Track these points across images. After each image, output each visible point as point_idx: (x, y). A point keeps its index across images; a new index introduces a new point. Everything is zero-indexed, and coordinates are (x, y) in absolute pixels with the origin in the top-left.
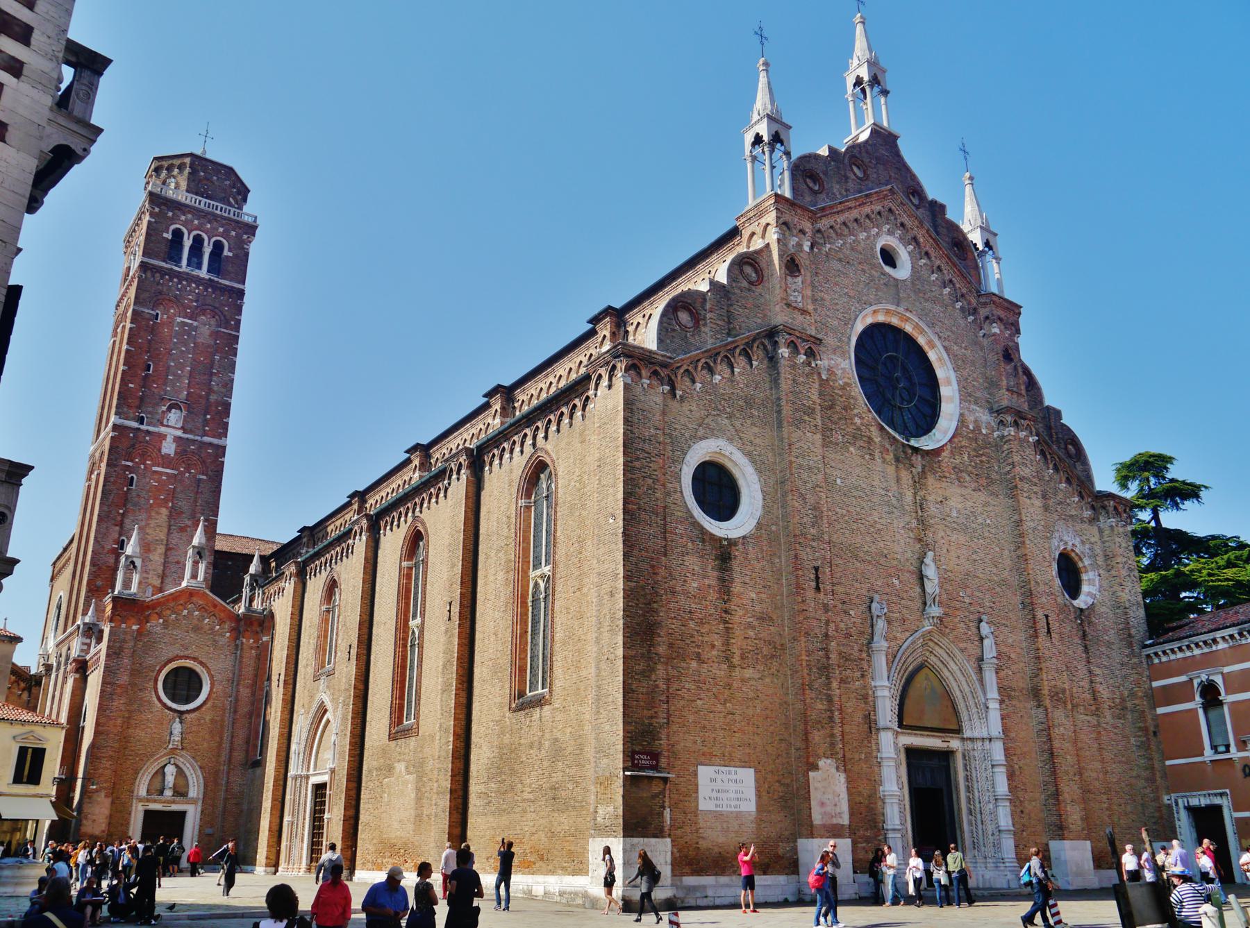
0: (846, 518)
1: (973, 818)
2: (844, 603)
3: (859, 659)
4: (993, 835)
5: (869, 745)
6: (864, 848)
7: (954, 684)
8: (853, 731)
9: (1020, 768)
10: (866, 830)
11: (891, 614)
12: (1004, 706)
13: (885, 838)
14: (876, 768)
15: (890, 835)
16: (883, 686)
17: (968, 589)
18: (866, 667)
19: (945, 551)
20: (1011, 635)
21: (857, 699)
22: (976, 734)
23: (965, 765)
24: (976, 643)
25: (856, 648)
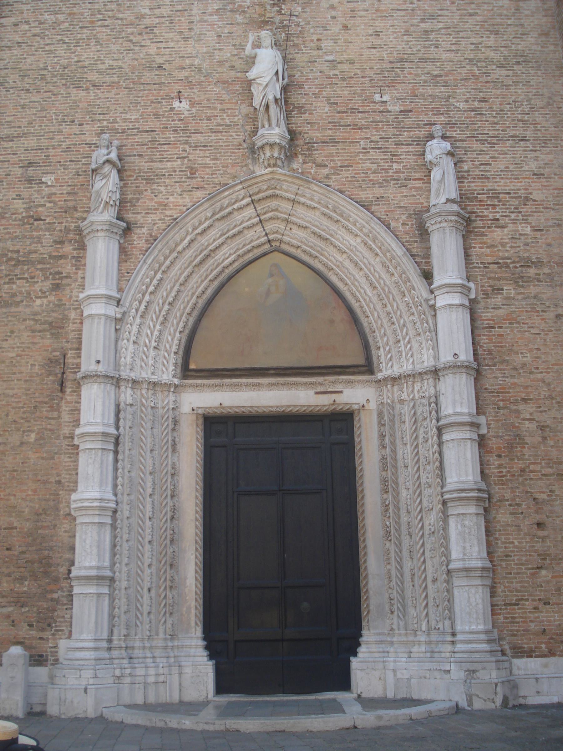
0: (67, 25)
1: (393, 547)
2: (31, 164)
3: (51, 257)
4: (435, 581)
5: (55, 414)
6: (8, 617)
7: (359, 276)
8: (11, 392)
9: (542, 428)
10: (21, 579)
11: (158, 165)
12: (498, 300)
13: (70, 596)
14: (65, 459)
15: (76, 590)
16: (89, 297)
17: (399, 87)
18: (67, 267)
19: (336, 29)
20: (533, 154)
21: (33, 331)
22: (408, 368)
23: (382, 436)
24: (418, 184)
25: (48, 239)
